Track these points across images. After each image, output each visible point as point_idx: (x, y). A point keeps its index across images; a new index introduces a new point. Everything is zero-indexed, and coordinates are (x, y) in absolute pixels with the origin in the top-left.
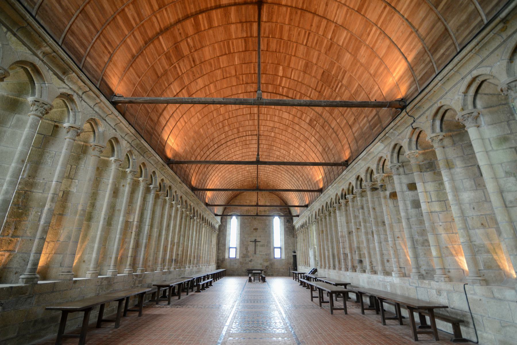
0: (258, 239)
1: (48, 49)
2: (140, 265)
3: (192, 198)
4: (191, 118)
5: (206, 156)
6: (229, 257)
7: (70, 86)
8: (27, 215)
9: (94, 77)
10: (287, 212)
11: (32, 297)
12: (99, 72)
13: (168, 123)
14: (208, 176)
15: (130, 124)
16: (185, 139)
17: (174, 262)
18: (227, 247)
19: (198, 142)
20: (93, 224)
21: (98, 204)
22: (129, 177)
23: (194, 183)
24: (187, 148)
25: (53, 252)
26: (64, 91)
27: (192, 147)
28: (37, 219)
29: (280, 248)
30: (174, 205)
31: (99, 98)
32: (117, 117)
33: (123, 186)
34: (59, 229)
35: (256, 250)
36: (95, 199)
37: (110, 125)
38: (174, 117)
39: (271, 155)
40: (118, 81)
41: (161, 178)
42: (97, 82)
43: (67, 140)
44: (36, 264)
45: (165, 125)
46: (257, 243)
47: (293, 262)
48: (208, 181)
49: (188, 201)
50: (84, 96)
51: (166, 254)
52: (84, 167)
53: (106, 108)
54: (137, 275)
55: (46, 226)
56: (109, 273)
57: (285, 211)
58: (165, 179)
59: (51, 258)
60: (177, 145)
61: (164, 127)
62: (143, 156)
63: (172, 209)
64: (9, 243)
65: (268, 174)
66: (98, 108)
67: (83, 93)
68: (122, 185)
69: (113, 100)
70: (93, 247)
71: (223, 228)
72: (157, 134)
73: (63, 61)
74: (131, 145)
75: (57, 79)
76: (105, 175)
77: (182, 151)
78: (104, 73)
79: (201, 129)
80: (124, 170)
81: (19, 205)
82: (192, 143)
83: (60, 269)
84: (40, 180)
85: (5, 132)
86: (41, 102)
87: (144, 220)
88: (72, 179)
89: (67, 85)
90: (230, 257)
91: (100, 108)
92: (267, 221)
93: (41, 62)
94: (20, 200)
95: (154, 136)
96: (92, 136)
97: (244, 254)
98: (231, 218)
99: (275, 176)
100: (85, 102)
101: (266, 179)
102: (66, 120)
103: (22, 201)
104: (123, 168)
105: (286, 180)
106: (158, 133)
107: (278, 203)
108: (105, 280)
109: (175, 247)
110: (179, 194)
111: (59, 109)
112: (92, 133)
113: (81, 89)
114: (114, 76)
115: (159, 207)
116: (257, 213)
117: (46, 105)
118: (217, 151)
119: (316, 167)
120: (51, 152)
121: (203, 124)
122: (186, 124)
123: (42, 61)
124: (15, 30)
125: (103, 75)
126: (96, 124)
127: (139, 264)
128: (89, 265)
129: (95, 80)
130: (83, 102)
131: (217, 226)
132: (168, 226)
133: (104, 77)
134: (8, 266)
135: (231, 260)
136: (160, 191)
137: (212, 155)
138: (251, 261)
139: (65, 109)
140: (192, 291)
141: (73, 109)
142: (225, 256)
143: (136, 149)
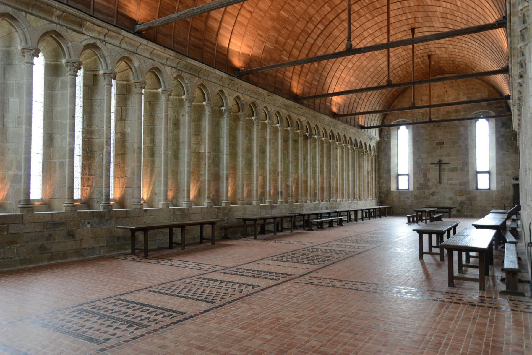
0: (445, 159)
1: (58, 12)
2: (224, 198)
3: (299, 111)
4: (257, 4)
5: (307, 45)
6: (398, 189)
7: (90, 35)
8: (94, 158)
9: (108, 15)
10: (502, 107)
11: (111, 219)
12: (111, 6)
13: (224, 24)
14: (325, 74)
15: (165, 47)
16: (258, 34)
17: (280, 195)
18: (393, 174)
19: (284, 32)
20: (157, 160)
21: (157, 140)
22: (187, 104)
23: (296, 88)
24: (268, 45)
25: (125, 186)
26: (86, 42)
27: (277, 42)
28: (101, 160)
29: (489, 172)
30: (268, 125)
31: (120, 34)
32: (147, 46)
33: (183, 115)
34: (124, 166)
35: (442, 177)
36: (154, 135)
37: (144, 56)
38: (229, 13)
39: (430, 14)
40: (136, 5)
41: (235, 96)
42: (113, 19)
43: (106, 86)
44: (108, 195)
45: (219, 29)
46: (444, 166)
47: (514, 196)
48: (328, 80)
49: (294, 116)
50: (107, 39)
51: (266, 185)
52: (132, 106)
53: (132, 41)
54: (219, 208)
55: (107, 166)
56: (184, 204)
57: (499, 107)
58: (240, 96)
59: (124, 191)
60: (249, 47)
61: (218, 31)
62: (198, 77)
64: (88, 181)
65: (445, 46)
66: (125, 44)
67: (105, 36)
68: (181, 115)
69: (136, 31)
70: (161, 181)
71: (384, 145)
72: (211, 45)
73: (74, 16)
74: (178, 69)
75: (77, 34)
76: (157, 109)
77: (261, 51)
78: (118, 5)
79: (282, 12)
80: (180, 98)
81: (87, 150)
82: (273, 36)
83: (133, 199)
84: (95, 128)
85: (57, 95)
86: (71, 62)
87: (222, 148)
88: (125, 120)
89: (87, 35)
90: (400, 188)
91: (127, 43)
92: (462, 129)
93: (58, 26)
94: (87, 146)
95: (205, 48)
96: (131, 73)
97: (421, 184)
98: (398, 129)
99: (458, 47)
100: (110, 44)
101: (446, 56)
102: (100, 67)
103: (88, 147)
104: (179, 96)
105: (479, 52)
106: (211, 43)
107: (484, 93)
108: (178, 210)
109: (280, 177)
110: (272, 109)
111: (92, 58)
112: (130, 70)
113: (101, 33)
114: (130, 2)
115: (241, 131)
116: (430, 118)
117: (75, 63)
118: (326, 33)
119: (466, 38)
120: (97, 101)
121: (282, 4)
122: (254, 14)
123: (59, 24)
124: (30, 11)
125: (118, 8)
126: (130, 60)
127: (223, 197)
128: (160, 197)
129: (110, 18)
130: (108, 45)
131: (373, 143)
132: (262, 151)
133: (119, 10)
134: (92, 198)
135: (399, 192)
136: (239, 111)
137: (319, 42)
138: (433, 194)
139: (96, 57)
140: (304, 229)
141: (101, 55)
142: (390, 188)
143: (185, 72)
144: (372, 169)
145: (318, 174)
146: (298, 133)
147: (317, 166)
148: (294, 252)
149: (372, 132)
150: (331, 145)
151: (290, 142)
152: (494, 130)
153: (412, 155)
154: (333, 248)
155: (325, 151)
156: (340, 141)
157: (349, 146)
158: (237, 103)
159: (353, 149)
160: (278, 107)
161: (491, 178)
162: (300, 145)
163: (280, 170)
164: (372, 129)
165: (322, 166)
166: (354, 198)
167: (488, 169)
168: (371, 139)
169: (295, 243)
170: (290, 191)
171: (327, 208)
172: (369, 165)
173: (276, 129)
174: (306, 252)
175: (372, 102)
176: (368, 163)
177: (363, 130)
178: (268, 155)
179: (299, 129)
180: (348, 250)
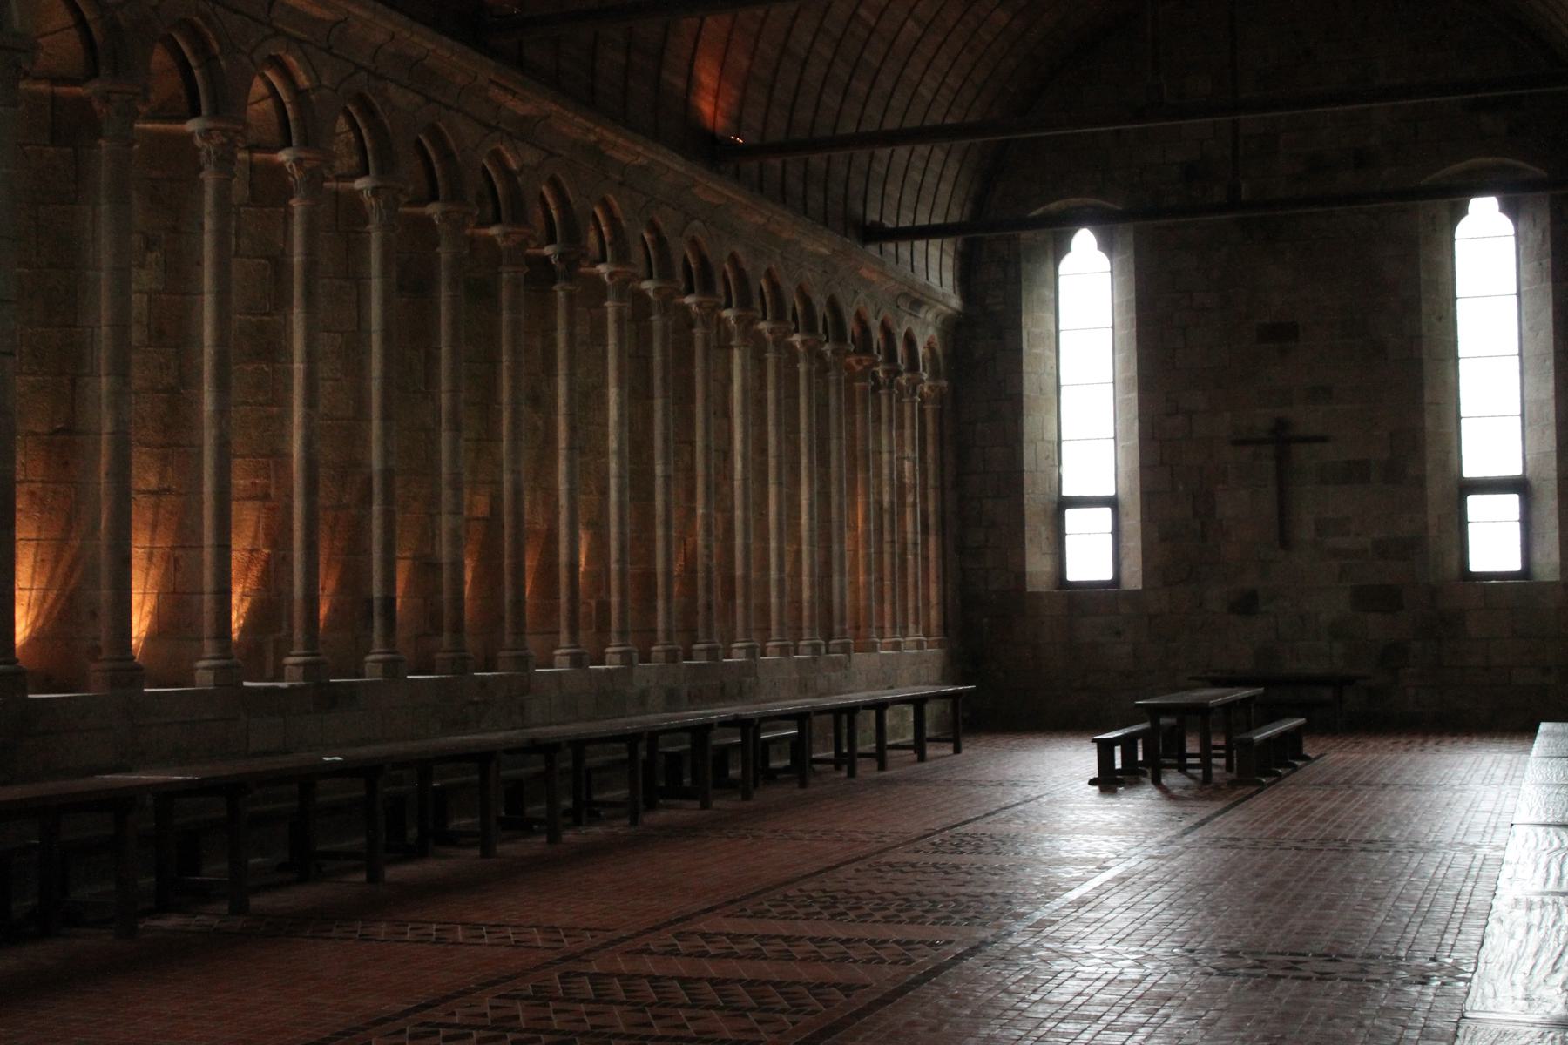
17: (377, 623)
18: (1034, 500)
63: (288, 215)
90: (1073, 575)
98: (1060, 248)
109: (376, 508)
115: (104, 207)
131: (926, 332)
136: (92, 73)
142: (1021, 575)
144: (924, 472)
145: (621, 491)
146: (492, 239)
147: (613, 445)
148: (437, 1015)
149: (919, 262)
150: (691, 326)
151: (444, 295)
152: (1547, 262)
153: (1134, 395)
154: (712, 969)
155: (657, 357)
156: (745, 303)
157: (796, 339)
158: (81, 23)
159: (821, 356)
160: (359, 68)
161: (1535, 513)
162: (505, 316)
163: (376, 464)
164: (920, 245)
165: (638, 446)
166: (829, 636)
167: (1514, 469)
168: (917, 304)
169: (460, 934)
170: (446, 596)
171: (672, 699)
172: (908, 451)
173: (349, 213)
174: (519, 1007)
175: (922, 90)
176: (901, 436)
177: (873, 249)
178: (298, 366)
179: (497, 220)
180: (805, 974)
